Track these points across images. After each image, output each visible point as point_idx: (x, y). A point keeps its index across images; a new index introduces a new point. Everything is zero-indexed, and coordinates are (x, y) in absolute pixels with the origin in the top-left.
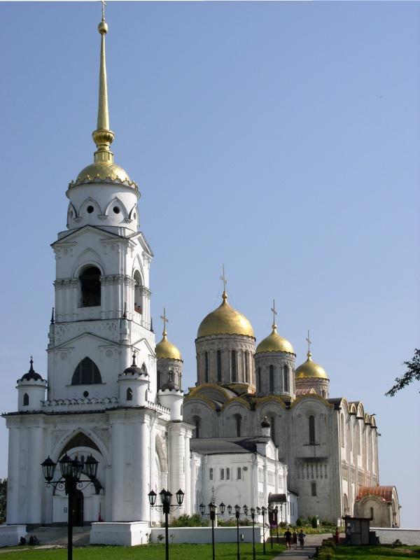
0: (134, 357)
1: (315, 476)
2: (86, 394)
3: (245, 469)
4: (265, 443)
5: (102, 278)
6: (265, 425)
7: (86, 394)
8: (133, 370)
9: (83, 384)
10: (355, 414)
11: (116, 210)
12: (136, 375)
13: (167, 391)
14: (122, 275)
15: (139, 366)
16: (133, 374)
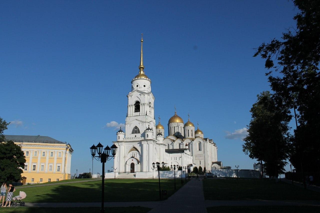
0: (149, 125)
1: (200, 159)
2: (136, 136)
3: (181, 157)
4: (187, 150)
5: (140, 104)
6: (186, 145)
7: (136, 136)
8: (149, 129)
9: (135, 133)
10: (211, 142)
11: (144, 86)
12: (149, 130)
13: (159, 136)
14: (146, 103)
15: (150, 128)
16: (148, 130)
